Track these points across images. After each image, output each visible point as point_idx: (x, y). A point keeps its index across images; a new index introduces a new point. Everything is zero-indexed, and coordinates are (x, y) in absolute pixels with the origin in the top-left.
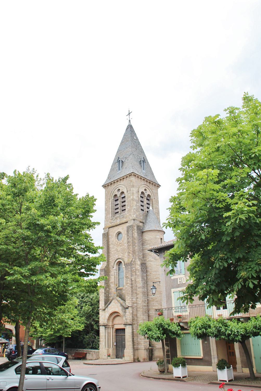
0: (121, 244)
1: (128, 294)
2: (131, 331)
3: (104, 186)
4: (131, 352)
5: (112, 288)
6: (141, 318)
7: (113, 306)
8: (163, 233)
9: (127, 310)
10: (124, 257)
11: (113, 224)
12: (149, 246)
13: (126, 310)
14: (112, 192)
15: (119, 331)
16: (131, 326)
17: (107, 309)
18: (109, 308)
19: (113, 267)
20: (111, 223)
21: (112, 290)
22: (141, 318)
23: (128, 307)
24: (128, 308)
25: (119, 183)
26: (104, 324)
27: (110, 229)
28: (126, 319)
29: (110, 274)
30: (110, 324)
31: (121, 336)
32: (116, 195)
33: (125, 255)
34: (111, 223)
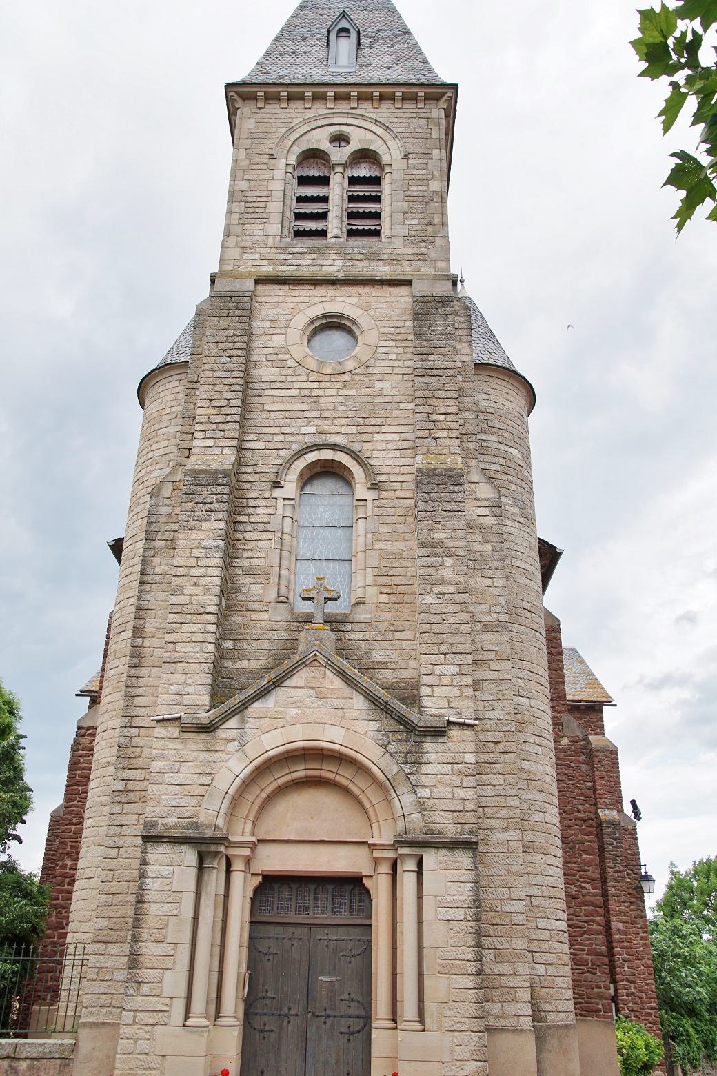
0: (346, 377)
1: (443, 648)
2: (464, 892)
3: (239, 95)
4: (463, 1052)
5: (256, 606)
6: (503, 813)
7: (293, 712)
8: (521, 401)
9: (429, 745)
10: (366, 446)
11: (283, 270)
12: (495, 439)
13: (419, 744)
14: (292, 130)
15: (276, 886)
16: (464, 859)
17: (233, 723)
18: (251, 722)
19: (276, 485)
20: (273, 262)
21: (254, 616)
22: (503, 813)
23: (449, 723)
24: (437, 733)
25: (366, 109)
26: (196, 826)
27: (260, 288)
28: (422, 807)
29: (243, 519)
30: (242, 833)
31: (299, 932)
32: (313, 155)
33: (376, 437)
34: (273, 262)
